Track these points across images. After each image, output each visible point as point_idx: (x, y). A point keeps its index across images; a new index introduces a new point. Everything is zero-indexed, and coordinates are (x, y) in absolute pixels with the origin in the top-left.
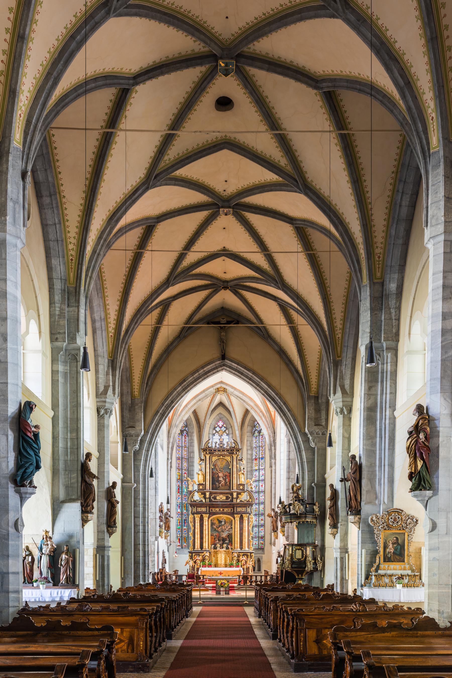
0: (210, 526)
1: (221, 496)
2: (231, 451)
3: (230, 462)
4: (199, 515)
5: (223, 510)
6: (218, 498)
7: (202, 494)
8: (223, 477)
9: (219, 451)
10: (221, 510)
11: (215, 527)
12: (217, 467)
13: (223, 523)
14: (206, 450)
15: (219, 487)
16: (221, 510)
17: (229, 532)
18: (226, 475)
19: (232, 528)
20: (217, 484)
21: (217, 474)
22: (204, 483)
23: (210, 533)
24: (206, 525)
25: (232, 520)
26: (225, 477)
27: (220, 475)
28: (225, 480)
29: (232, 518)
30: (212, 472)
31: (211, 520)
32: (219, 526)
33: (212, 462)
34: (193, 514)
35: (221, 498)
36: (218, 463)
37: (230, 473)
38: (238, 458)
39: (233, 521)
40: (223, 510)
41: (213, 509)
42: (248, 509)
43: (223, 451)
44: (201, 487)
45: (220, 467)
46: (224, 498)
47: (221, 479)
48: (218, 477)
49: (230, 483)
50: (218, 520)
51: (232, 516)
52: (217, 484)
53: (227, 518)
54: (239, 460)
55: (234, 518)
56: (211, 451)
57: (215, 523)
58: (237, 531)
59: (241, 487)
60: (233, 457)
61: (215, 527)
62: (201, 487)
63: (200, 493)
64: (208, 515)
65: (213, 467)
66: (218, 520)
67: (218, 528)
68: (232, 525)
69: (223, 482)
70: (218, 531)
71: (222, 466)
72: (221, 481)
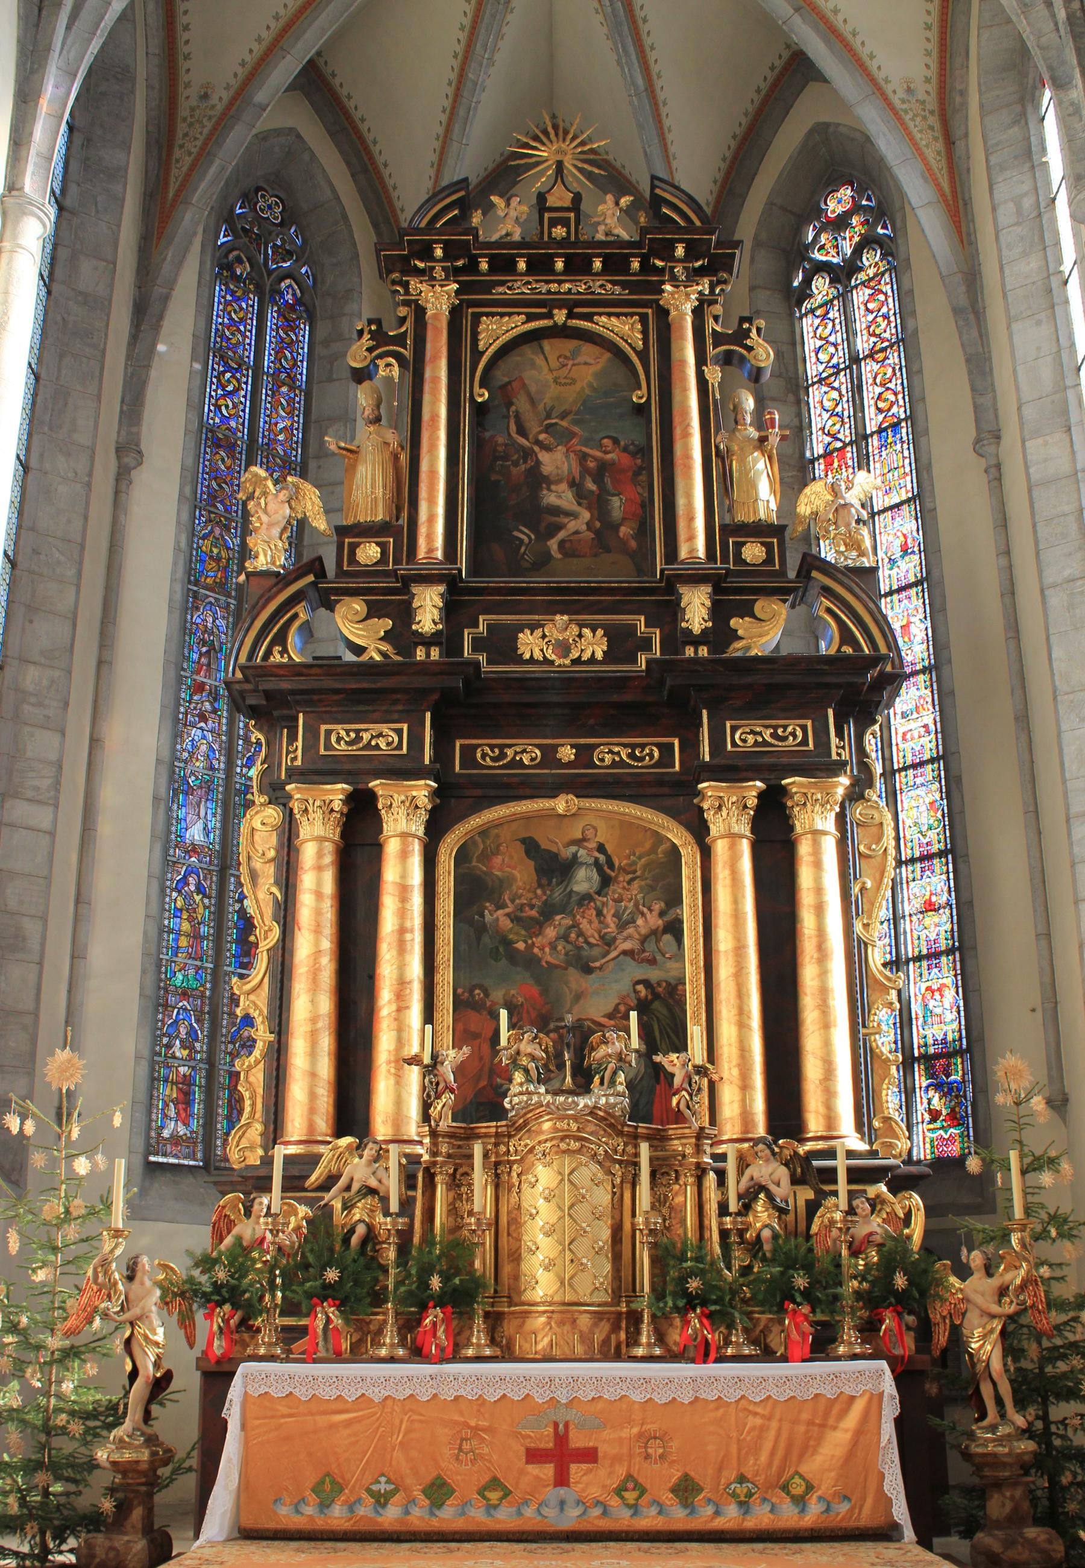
0: (446, 905)
1: (559, 628)
2: (647, 267)
3: (643, 355)
4: (337, 793)
5: (584, 754)
6: (530, 644)
7: (374, 611)
8: (575, 485)
9: (540, 266)
10: (567, 753)
11: (498, 918)
12: (521, 404)
13: (584, 880)
14: (426, 253)
15: (547, 557)
16: (567, 753)
17: (653, 974)
18: (604, 467)
19: (675, 929)
20: (524, 534)
21: (527, 454)
22: (404, 521)
23: (445, 977)
24: (404, 891)
25: (675, 853)
26: (598, 478)
27: (553, 462)
28: (599, 504)
29: (677, 835)
30: (478, 445)
31: (462, 856)
32: (548, 912)
33: (477, 355)
34: (277, 794)
35: (564, 648)
36: (529, 375)
37: (644, 451)
38: (711, 325)
39: (689, 855)
40: (584, 754)
41: (485, 750)
42: (834, 740)
43: (578, 266)
44: (369, 552)
45: (547, 399)
46: (594, 645)
47: (561, 497)
48: (537, 480)
49: (644, 530)
50: (531, 847)
51: (673, 813)
52: (524, 534)
53: (627, 826)
54: (719, 339)
55: (699, 830)
56: (472, 267)
57: (504, 883)
58: (739, 950)
59: (753, 552)
60: (663, 313)
61: (498, 918)
62: (369, 552)
63: (358, 606)
64: (422, 790)
65: (483, 396)
66: (531, 847)
67: (534, 927)
68: (674, 898)
69: (580, 522)
70: (530, 962)
71: (570, 396)
72: (556, 511)
